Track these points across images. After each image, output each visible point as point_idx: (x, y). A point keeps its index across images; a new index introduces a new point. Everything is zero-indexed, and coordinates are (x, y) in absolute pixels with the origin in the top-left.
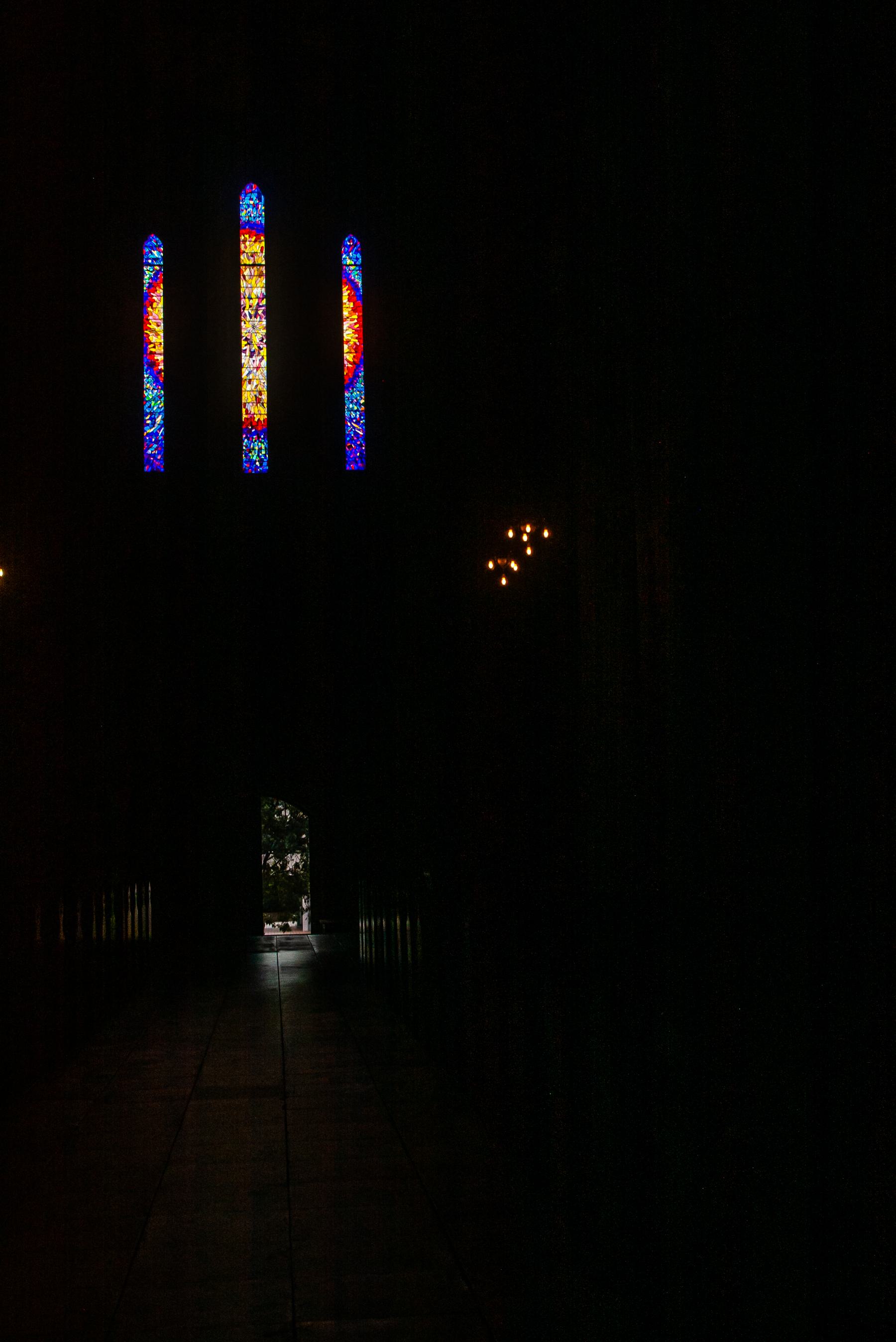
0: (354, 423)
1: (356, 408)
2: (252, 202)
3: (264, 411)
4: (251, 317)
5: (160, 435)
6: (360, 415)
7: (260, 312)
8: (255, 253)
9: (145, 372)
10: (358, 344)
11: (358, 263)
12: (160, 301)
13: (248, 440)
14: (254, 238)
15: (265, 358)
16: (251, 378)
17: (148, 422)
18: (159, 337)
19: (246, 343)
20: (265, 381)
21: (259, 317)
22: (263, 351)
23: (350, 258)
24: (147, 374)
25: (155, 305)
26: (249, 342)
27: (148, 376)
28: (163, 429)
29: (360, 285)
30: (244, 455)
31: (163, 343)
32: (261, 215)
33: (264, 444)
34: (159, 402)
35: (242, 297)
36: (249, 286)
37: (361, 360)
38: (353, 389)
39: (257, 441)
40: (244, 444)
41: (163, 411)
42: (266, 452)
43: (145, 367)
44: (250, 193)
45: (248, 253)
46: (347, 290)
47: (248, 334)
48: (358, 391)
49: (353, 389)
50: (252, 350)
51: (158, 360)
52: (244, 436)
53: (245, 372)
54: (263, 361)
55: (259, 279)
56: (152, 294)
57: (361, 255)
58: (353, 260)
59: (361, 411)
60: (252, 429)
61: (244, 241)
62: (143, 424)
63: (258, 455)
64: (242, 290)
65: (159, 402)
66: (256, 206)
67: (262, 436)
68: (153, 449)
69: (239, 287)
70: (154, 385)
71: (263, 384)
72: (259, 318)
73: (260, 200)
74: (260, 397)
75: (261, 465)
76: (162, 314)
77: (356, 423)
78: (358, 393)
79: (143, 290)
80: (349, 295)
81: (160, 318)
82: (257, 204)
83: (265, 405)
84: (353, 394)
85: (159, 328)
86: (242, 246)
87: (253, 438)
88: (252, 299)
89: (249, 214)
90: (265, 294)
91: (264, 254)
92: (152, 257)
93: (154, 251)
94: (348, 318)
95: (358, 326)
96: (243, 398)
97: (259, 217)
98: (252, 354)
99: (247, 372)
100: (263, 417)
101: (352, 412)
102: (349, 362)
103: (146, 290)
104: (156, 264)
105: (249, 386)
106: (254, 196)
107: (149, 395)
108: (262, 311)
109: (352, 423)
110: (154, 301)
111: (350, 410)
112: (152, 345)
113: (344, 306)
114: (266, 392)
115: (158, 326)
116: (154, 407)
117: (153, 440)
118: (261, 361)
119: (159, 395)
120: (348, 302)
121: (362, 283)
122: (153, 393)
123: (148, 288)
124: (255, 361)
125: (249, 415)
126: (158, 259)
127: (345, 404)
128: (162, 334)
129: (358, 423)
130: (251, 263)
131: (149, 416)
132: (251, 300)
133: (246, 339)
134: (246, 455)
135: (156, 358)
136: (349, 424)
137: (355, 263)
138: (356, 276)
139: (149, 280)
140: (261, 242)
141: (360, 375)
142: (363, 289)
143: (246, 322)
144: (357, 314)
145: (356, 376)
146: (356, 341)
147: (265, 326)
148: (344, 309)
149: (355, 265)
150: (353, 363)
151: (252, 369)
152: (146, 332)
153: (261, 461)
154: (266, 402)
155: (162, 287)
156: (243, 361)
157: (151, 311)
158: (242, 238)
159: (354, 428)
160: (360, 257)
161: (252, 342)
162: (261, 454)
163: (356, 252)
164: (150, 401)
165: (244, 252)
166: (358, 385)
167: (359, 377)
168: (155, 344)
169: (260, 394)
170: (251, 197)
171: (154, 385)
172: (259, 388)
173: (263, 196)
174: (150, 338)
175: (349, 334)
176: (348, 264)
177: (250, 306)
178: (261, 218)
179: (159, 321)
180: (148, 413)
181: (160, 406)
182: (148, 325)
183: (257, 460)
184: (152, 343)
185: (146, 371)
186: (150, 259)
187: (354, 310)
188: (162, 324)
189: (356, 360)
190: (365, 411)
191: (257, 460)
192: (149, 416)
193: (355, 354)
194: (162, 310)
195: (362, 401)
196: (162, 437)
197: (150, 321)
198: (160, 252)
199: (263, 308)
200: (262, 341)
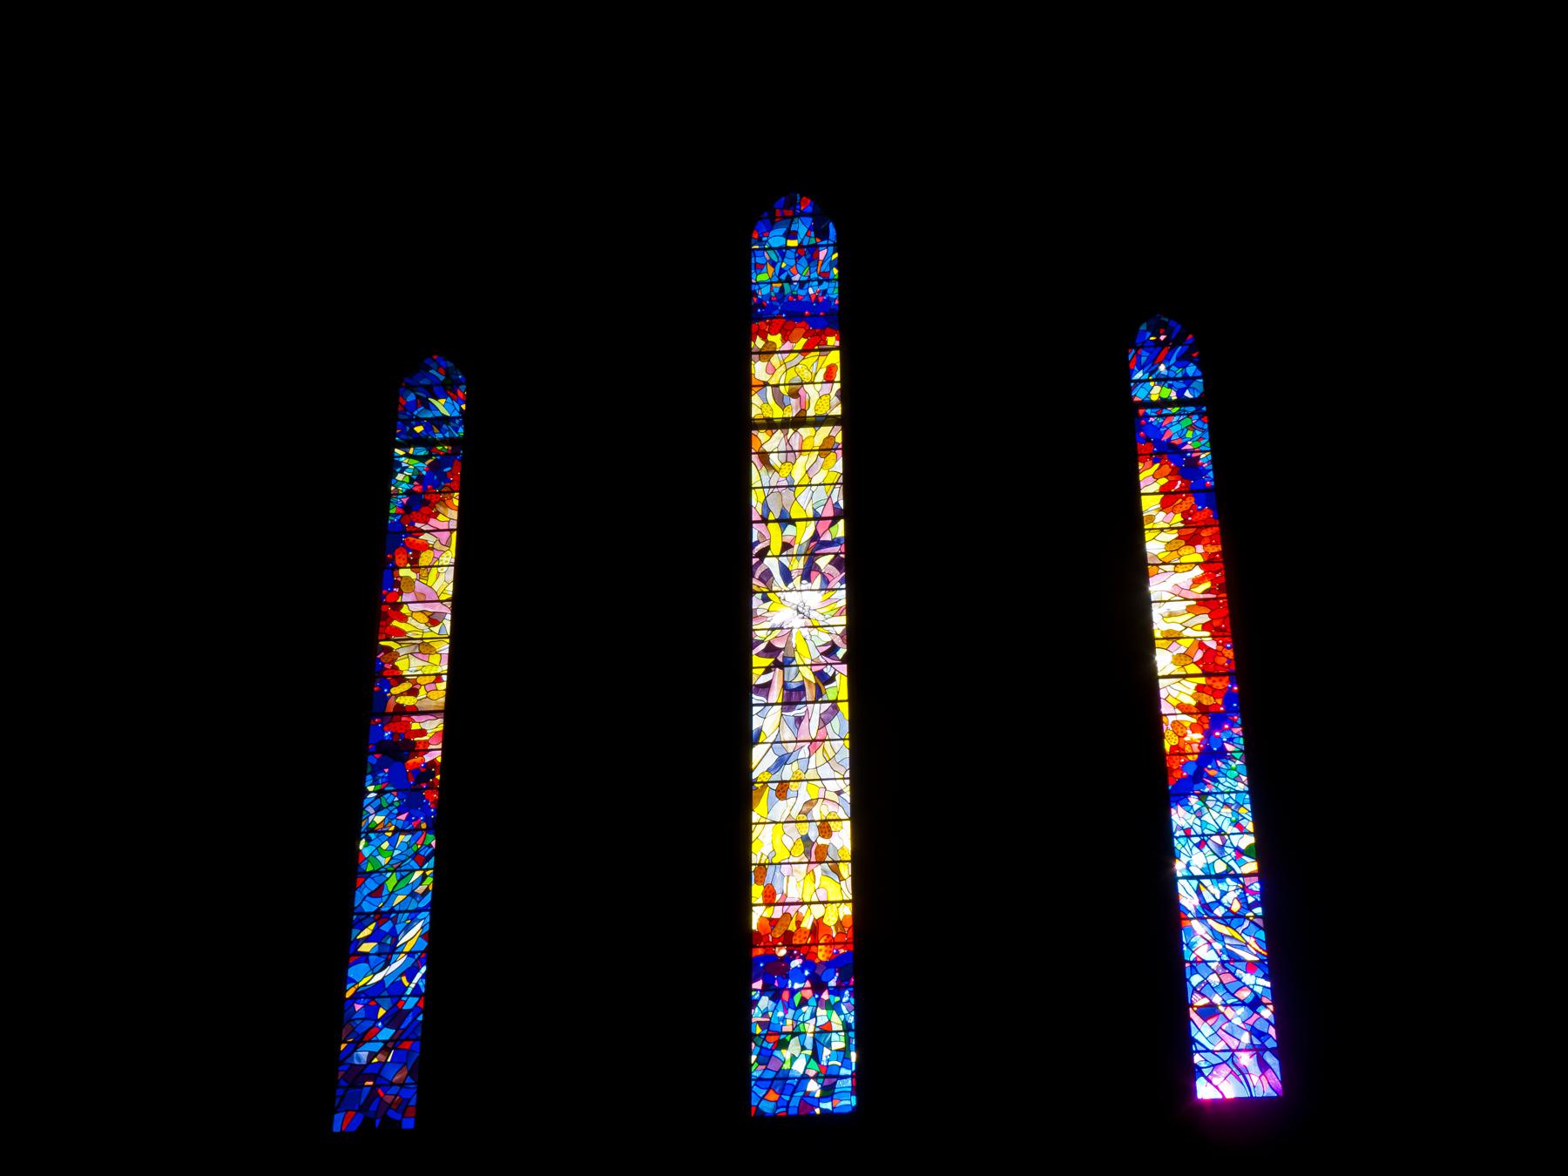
0: (1215, 918)
1: (1220, 867)
2: (793, 243)
3: (842, 889)
4: (787, 576)
5: (408, 992)
6: (1245, 889)
7: (823, 562)
8: (802, 384)
9: (369, 777)
10: (1212, 644)
11: (1187, 394)
12: (448, 545)
13: (776, 998)
14: (802, 342)
15: (844, 708)
16: (786, 777)
17: (366, 948)
18: (435, 659)
19: (768, 662)
20: (845, 786)
21: (819, 577)
22: (833, 684)
23: (1161, 380)
24: (375, 783)
25: (425, 558)
26: (780, 659)
27: (379, 787)
28: (424, 969)
29: (1205, 457)
30: (754, 1058)
31: (445, 678)
32: (825, 277)
33: (840, 1013)
34: (418, 874)
35: (755, 517)
36: (785, 483)
37: (1228, 697)
38: (1202, 796)
39: (812, 1002)
40: (756, 1015)
41: (431, 903)
42: (848, 1041)
43: (373, 759)
44: (787, 218)
45: (777, 386)
46: (1155, 477)
47: (777, 633)
48: (1226, 804)
49: (1202, 796)
50: (794, 686)
51: (423, 732)
52: (758, 985)
53: (761, 759)
54: (835, 721)
55: (821, 460)
56: (418, 525)
57: (1199, 367)
58: (1170, 386)
59: (1244, 876)
60: (790, 957)
61: (767, 353)
62: (347, 953)
63: (816, 1056)
64: (757, 499)
65: (418, 874)
66: (809, 252)
67: (832, 983)
68: (376, 1047)
69: (745, 488)
70: (403, 817)
71: (835, 797)
72: (817, 582)
73: (822, 233)
74: (821, 841)
75: (828, 1092)
76: (451, 588)
77: (1223, 920)
78: (1226, 811)
79: (389, 514)
80: (1164, 491)
81: (443, 597)
82: (814, 249)
83: (846, 870)
84: (1207, 818)
85: (436, 629)
86: (759, 370)
87: (793, 992)
88: (793, 522)
89: (783, 277)
90: (841, 503)
91: (837, 386)
92: (430, 415)
93: (437, 399)
94: (1164, 563)
95: (1207, 585)
96: (755, 847)
97: (820, 283)
98: (793, 697)
99: (771, 759)
100: (838, 914)
101: (1207, 882)
102: (1184, 709)
103: (395, 515)
104: (439, 436)
105: (781, 804)
106: (801, 228)
107: (375, 853)
108: (832, 556)
109: (1210, 921)
110: (426, 546)
111: (1197, 872)
112: (406, 686)
113: (1146, 527)
114: (847, 825)
115: (433, 621)
116: (392, 893)
117: (381, 1012)
118: (824, 721)
119: (417, 853)
120: (1162, 514)
121: (1213, 451)
122: (393, 845)
123: (407, 508)
124: (804, 723)
125: (779, 909)
126: (444, 419)
127: (1171, 855)
128: (444, 647)
129: (1230, 918)
130: (791, 413)
131: (372, 926)
132: (790, 528)
133: (771, 650)
134: (766, 1057)
135: (415, 726)
136: (1195, 924)
137: (1180, 393)
138: (1189, 434)
139: (412, 480)
140: (827, 350)
141: (1229, 747)
142: (1214, 470)
143: (770, 595)
144: (1200, 548)
145: (1211, 755)
146: (1208, 634)
147: (843, 603)
148: (1148, 536)
149: (1182, 401)
150: (1201, 709)
151: (790, 747)
152: (382, 643)
153: (829, 1080)
154: (849, 858)
155: (456, 502)
156: (756, 723)
157: (408, 578)
158: (759, 343)
159: (1220, 937)
160: (1199, 373)
161: (794, 659)
162: (826, 1052)
163: (1183, 361)
164: (380, 871)
165: (766, 384)
166: (1225, 783)
167: (1222, 754)
168: (415, 683)
169: (825, 828)
170: (789, 229)
171: (403, 817)
172: (818, 813)
173: (831, 224)
174: (402, 664)
175: (1171, 615)
176: (1154, 398)
177: (786, 546)
178: (825, 285)
179: (438, 608)
180: (368, 914)
181: (420, 890)
182: (395, 623)
183: (811, 1073)
184: (401, 679)
185: (374, 774)
186: (419, 421)
187: (1190, 537)
188: (449, 617)
189: (1208, 700)
190: (1261, 875)
191: (811, 1073)
192: (372, 926)
193: (1202, 680)
194: (449, 574)
195: (1247, 841)
196: (416, 999)
197: (404, 610)
198: (456, 399)
199: (836, 549)
200: (831, 650)
